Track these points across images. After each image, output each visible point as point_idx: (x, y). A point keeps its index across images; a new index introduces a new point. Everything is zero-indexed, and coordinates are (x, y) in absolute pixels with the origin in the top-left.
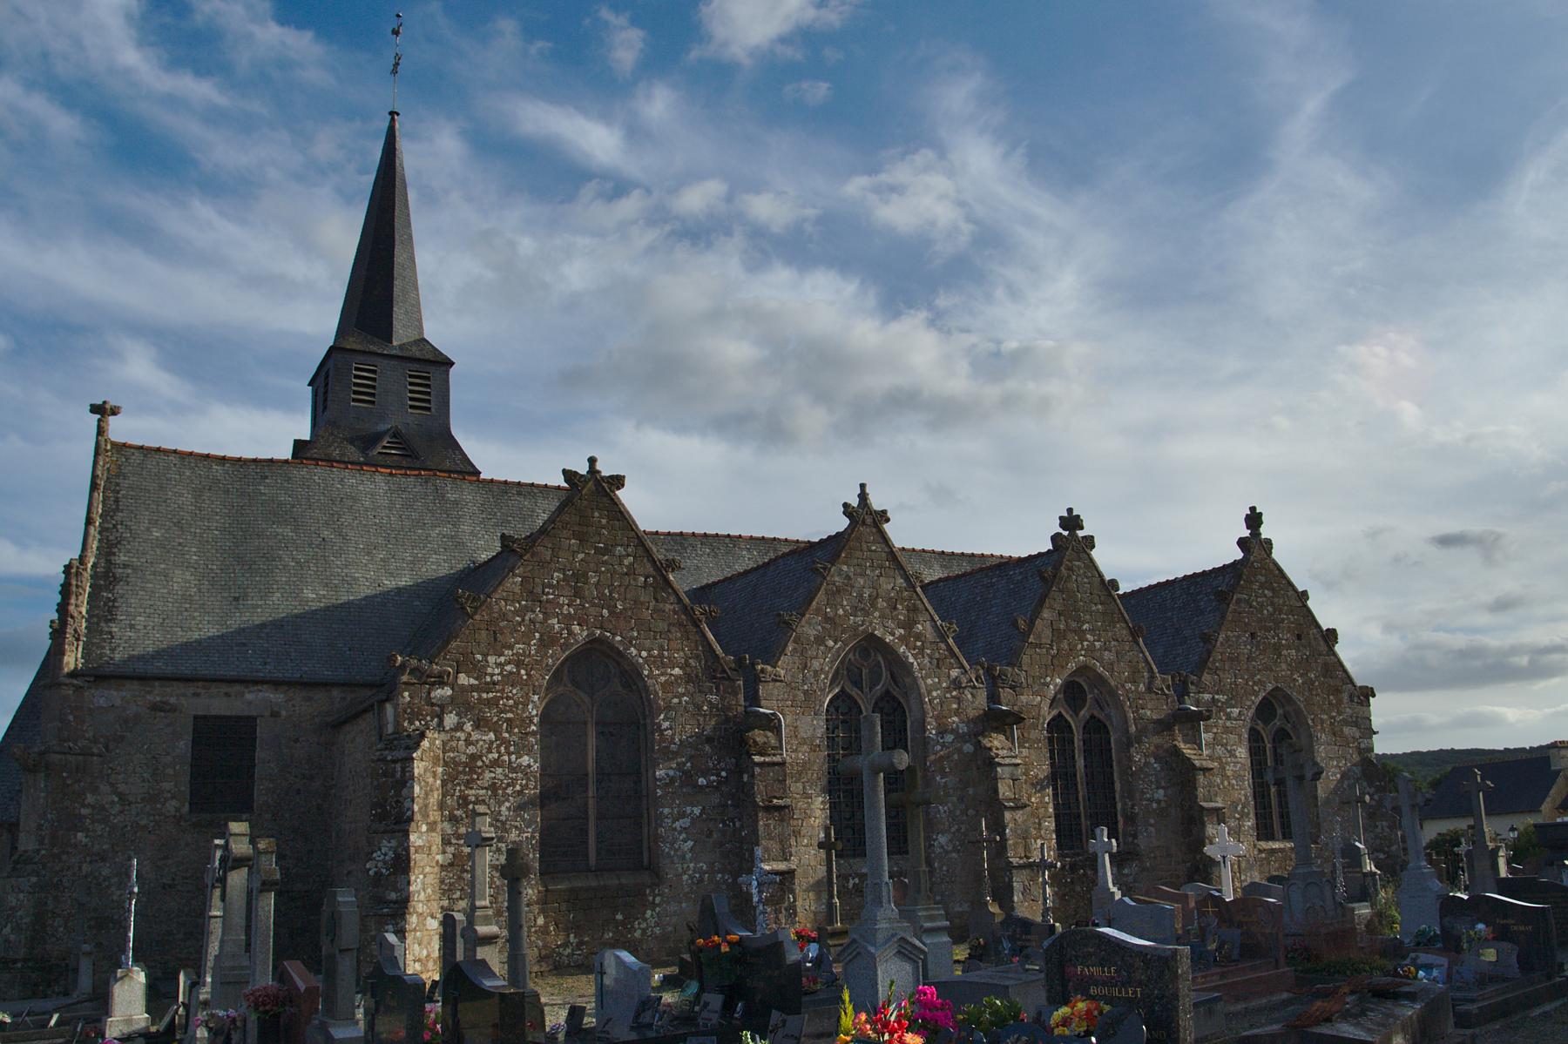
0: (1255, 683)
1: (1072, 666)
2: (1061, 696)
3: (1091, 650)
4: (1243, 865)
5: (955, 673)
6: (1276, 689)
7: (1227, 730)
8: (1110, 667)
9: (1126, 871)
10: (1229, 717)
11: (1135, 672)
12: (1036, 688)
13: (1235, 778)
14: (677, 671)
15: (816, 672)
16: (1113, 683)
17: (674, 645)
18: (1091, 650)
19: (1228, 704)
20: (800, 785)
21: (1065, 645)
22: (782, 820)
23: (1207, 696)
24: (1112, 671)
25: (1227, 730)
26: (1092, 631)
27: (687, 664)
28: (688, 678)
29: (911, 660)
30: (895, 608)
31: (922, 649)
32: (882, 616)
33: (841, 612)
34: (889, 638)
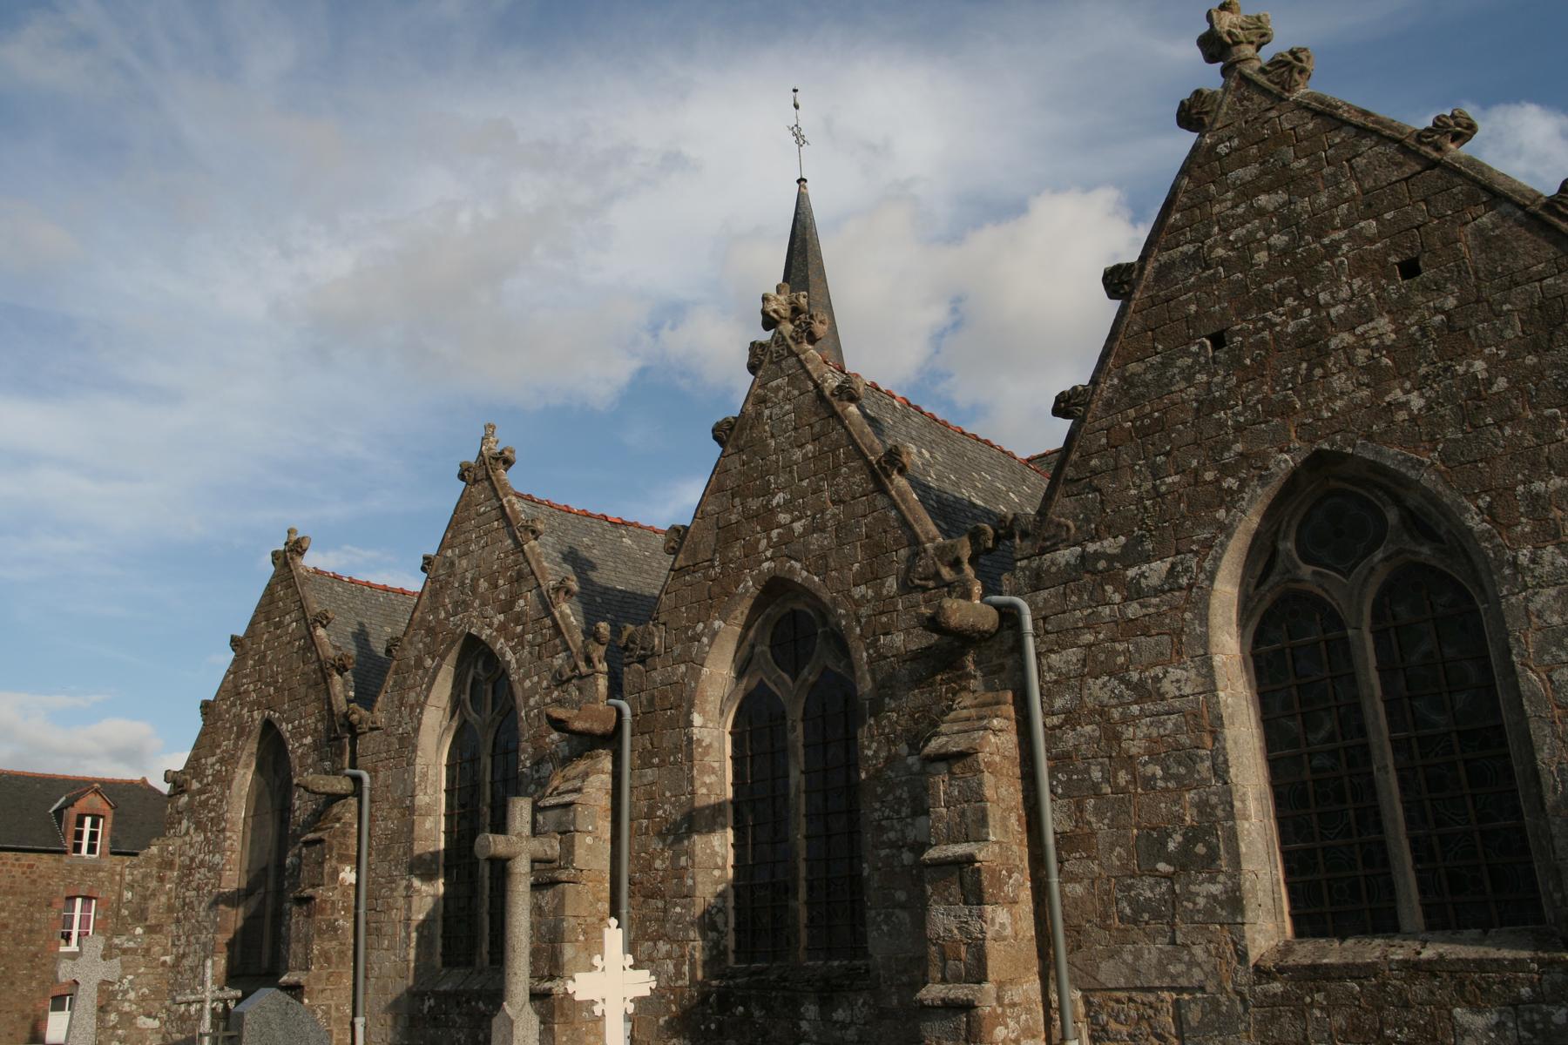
0: (1225, 470)
1: (749, 586)
2: (763, 648)
3: (787, 538)
4: (1194, 1016)
5: (558, 661)
6: (1317, 461)
7: (1129, 628)
8: (820, 564)
9: (840, 1015)
10: (1134, 592)
11: (876, 551)
12: (678, 649)
13: (1154, 757)
14: (308, 740)
15: (412, 707)
16: (826, 596)
17: (310, 709)
18: (787, 538)
19: (1133, 554)
20: (386, 865)
21: (737, 550)
22: (308, 916)
23: (1066, 555)
24: (823, 571)
25: (1129, 628)
26: (787, 506)
27: (316, 730)
28: (316, 747)
29: (509, 656)
30: (496, 587)
31: (521, 636)
32: (483, 604)
33: (443, 615)
34: (485, 634)
